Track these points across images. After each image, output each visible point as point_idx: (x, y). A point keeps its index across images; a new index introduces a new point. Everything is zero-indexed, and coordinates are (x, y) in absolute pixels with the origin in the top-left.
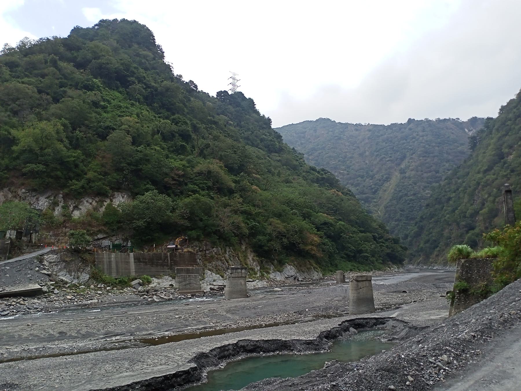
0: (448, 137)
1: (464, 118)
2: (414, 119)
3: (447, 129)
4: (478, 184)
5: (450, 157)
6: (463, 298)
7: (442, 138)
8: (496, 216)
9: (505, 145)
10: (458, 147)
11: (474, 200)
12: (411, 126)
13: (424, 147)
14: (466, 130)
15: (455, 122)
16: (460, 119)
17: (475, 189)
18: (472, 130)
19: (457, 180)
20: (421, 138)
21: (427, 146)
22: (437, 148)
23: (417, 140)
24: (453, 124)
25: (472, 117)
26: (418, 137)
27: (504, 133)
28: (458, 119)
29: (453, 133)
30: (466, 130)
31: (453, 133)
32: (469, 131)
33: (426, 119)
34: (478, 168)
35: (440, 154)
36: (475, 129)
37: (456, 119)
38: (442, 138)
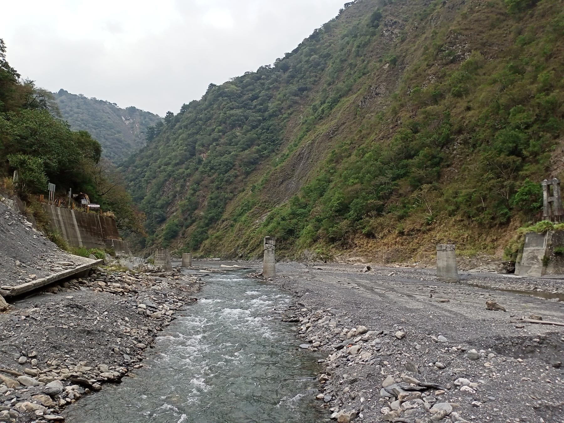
0: (105, 121)
1: (123, 105)
2: (67, 91)
3: (104, 112)
4: (170, 176)
5: (108, 144)
6: (559, 259)
7: (99, 120)
8: (196, 209)
9: (198, 143)
10: (115, 134)
11: (164, 191)
12: (63, 97)
13: (80, 126)
14: (124, 119)
15: (113, 107)
16: (118, 105)
17: (166, 180)
18: (129, 120)
19: (134, 168)
20: (76, 115)
21: (83, 126)
22: (94, 130)
23: (71, 116)
24: (110, 108)
25: (130, 106)
26: (71, 113)
27: (195, 131)
28: (116, 105)
29: (109, 118)
30: (124, 119)
31: (109, 118)
32: (126, 119)
33: (81, 95)
34: (165, 160)
35: (97, 137)
36: (133, 119)
37: (114, 104)
38: (99, 120)
